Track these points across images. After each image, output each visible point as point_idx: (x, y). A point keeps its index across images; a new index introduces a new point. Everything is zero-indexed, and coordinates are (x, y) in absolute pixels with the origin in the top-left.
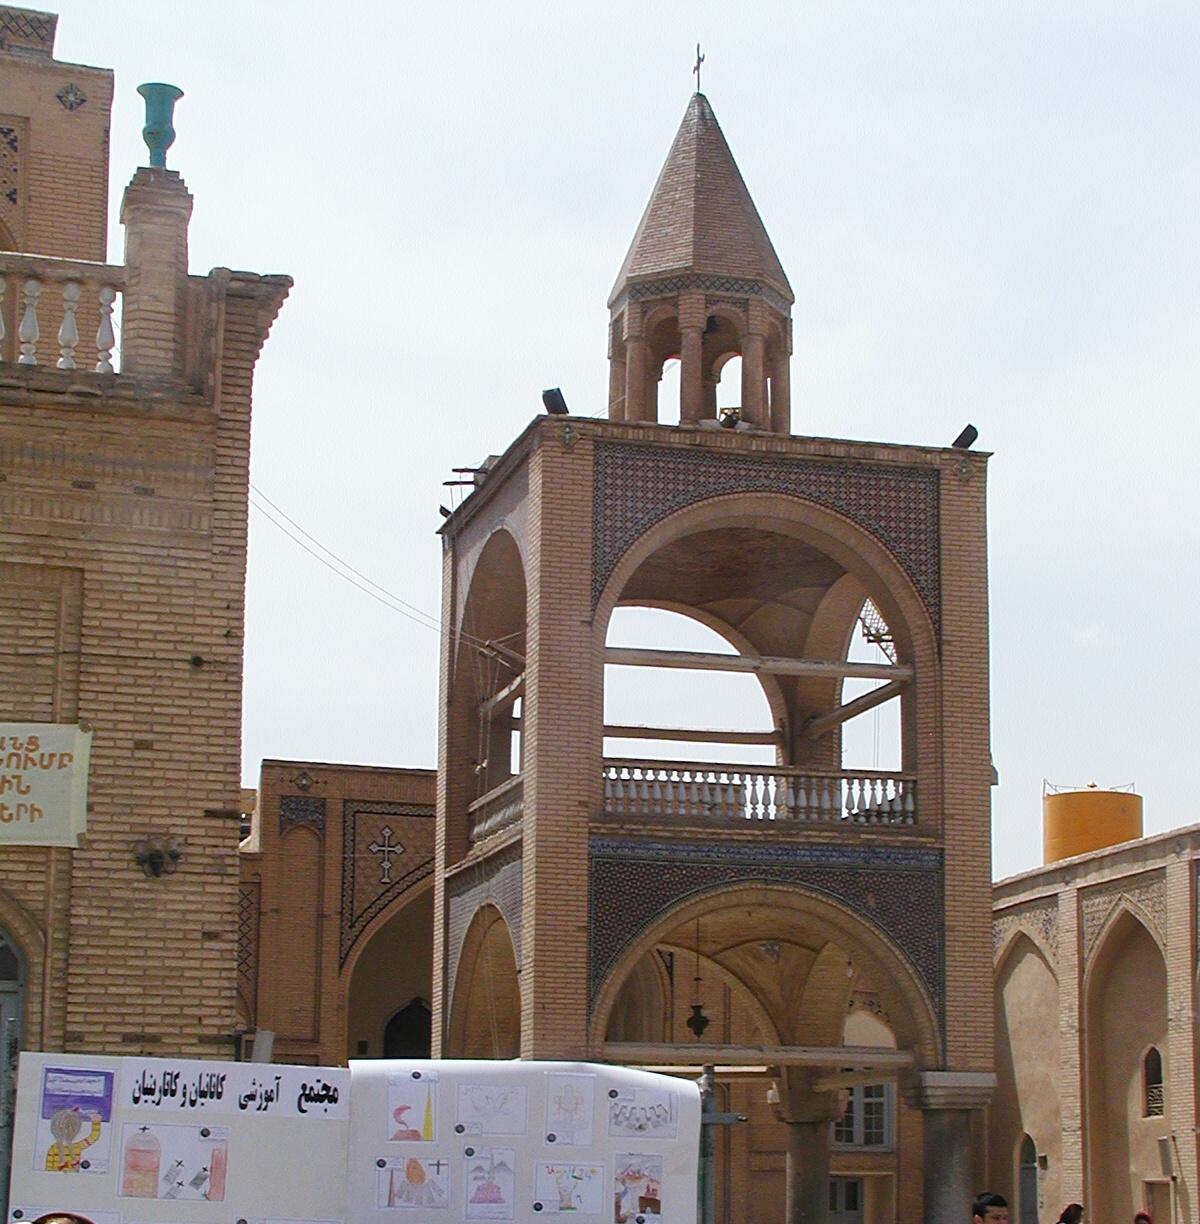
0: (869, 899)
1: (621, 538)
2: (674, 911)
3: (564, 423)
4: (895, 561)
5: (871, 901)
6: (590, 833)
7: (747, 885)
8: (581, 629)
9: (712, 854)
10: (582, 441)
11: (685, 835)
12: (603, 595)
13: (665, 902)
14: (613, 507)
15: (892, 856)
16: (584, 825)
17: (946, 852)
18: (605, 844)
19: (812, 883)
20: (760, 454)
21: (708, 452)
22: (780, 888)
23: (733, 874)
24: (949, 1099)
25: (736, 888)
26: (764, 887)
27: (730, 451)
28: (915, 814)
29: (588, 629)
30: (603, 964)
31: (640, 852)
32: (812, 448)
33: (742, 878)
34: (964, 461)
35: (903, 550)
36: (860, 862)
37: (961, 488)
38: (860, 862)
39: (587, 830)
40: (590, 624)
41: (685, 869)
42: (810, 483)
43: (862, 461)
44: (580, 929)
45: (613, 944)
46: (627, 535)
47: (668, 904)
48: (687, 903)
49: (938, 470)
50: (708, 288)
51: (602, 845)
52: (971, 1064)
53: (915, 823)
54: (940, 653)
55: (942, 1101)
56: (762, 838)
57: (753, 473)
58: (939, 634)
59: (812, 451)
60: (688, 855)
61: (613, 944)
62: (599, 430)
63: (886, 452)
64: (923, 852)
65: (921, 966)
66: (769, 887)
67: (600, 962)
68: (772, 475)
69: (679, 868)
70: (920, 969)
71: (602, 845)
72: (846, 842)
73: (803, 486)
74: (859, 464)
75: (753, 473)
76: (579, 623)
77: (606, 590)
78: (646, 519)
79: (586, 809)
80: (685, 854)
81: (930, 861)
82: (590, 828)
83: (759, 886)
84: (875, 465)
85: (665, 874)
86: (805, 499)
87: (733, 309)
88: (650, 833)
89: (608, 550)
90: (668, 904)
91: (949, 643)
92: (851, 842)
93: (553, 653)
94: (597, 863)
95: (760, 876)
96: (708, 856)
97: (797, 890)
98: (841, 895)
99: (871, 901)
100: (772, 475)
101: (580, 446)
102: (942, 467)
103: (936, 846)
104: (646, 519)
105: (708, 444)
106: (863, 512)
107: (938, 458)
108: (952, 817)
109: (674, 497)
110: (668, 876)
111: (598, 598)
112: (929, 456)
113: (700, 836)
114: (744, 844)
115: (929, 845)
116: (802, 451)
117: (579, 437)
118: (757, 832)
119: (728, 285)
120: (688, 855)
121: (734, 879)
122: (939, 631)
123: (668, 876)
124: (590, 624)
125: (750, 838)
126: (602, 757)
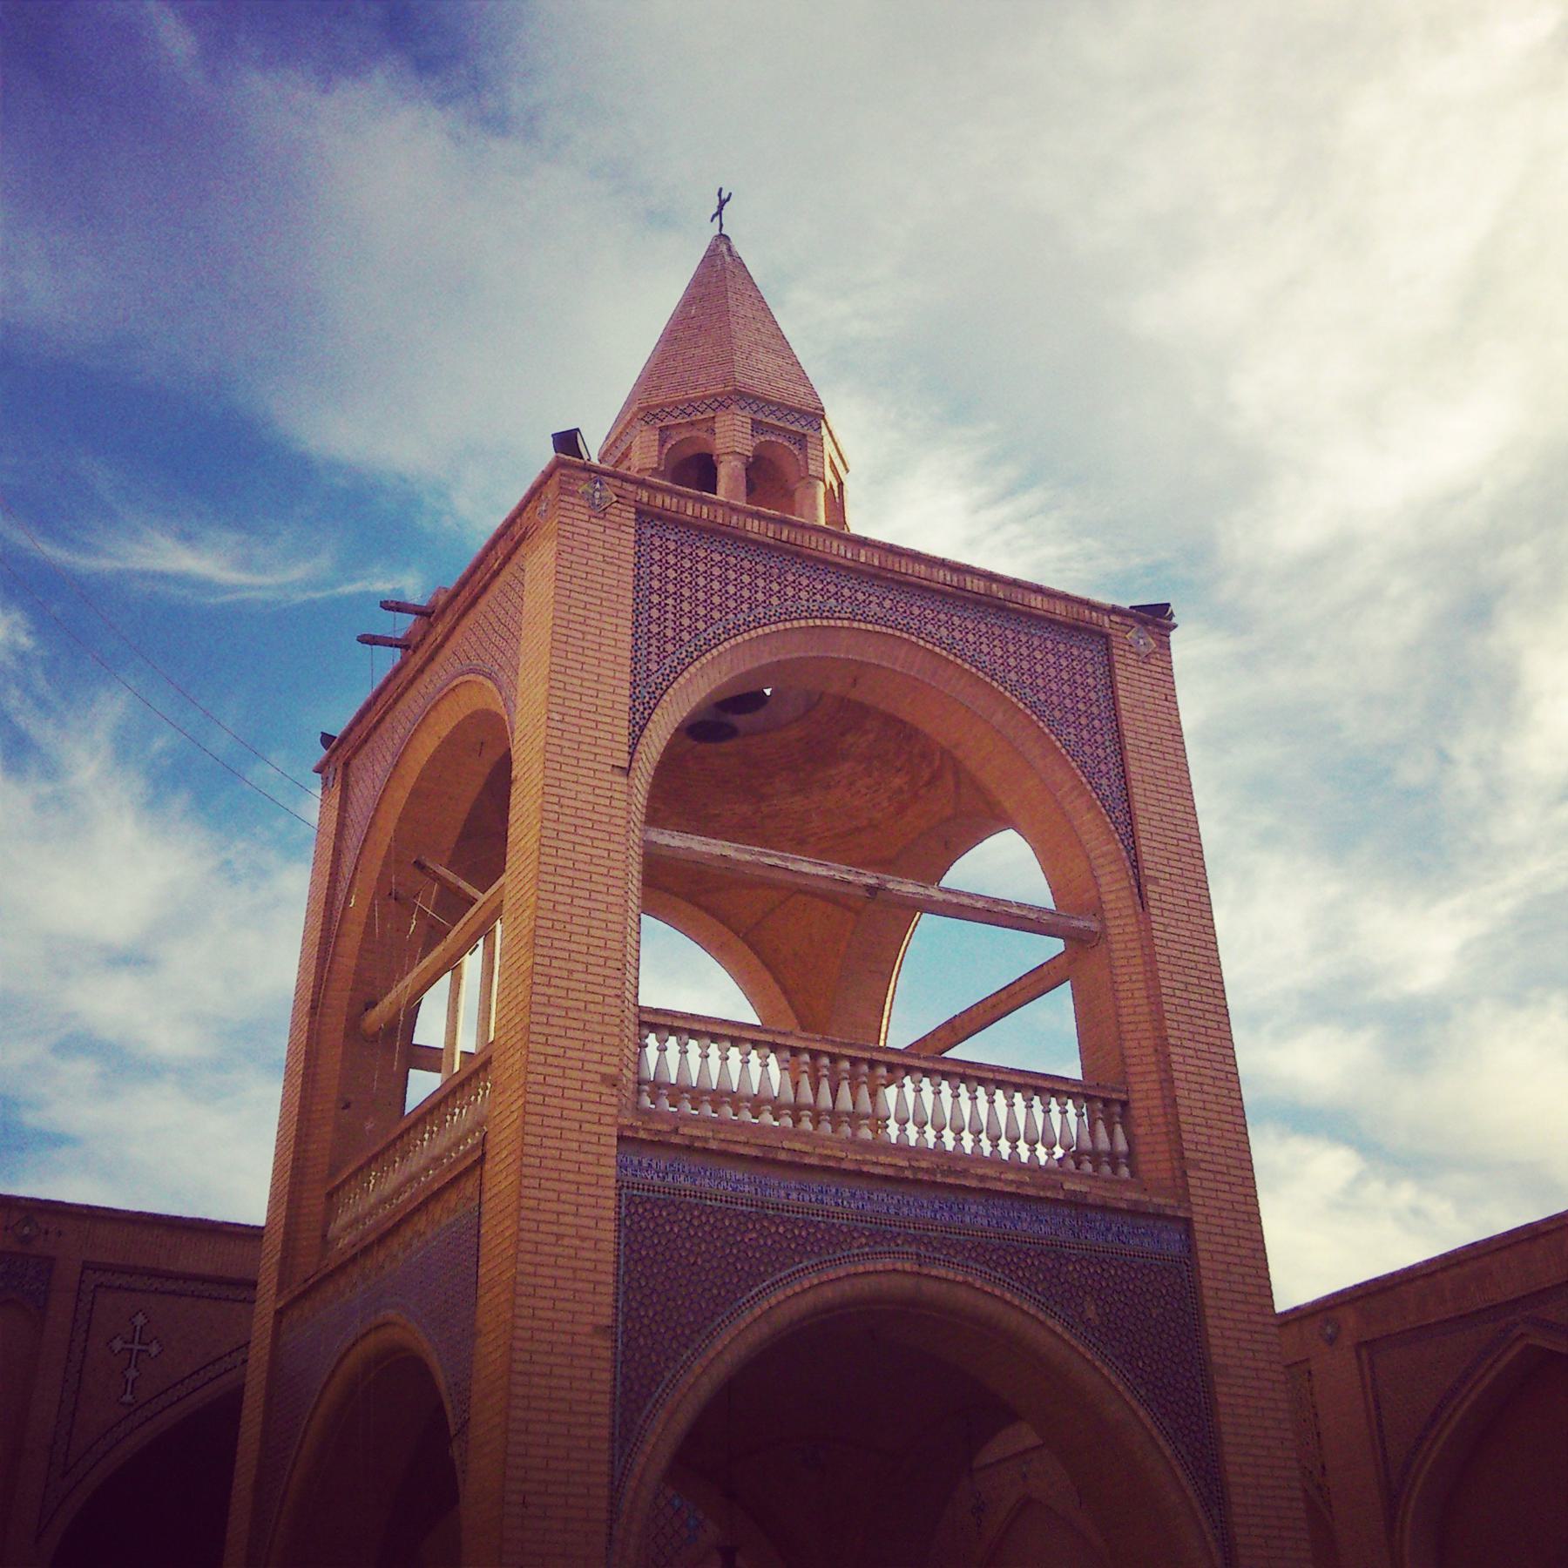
0: (1086, 1305)
1: (674, 653)
2: (765, 1306)
4: (1063, 751)
5: (1091, 1312)
6: (620, 1138)
8: (610, 777)
12: (646, 732)
14: (662, 607)
15: (1114, 1229)
16: (608, 1120)
17: (1197, 1226)
18: (645, 1165)
20: (873, 571)
22: (942, 1272)
23: (863, 1240)
26: (916, 1268)
28: (1130, 1155)
29: (624, 780)
35: (1072, 737)
39: (614, 1131)
40: (627, 771)
41: (783, 1222)
47: (756, 1290)
51: (640, 1163)
53: (1132, 1174)
54: (1141, 895)
57: (861, 597)
58: (1137, 867)
59: (941, 579)
64: (1159, 1224)
71: (640, 1163)
72: (1042, 1194)
73: (929, 626)
76: (609, 769)
77: (650, 725)
79: (615, 1091)
82: (621, 1127)
83: (907, 1267)
87: (786, 444)
88: (724, 1146)
89: (653, 667)
90: (756, 1290)
92: (1049, 1194)
99: (1091, 1312)
100: (887, 604)
103: (1181, 1214)
104: (710, 630)
106: (1013, 676)
109: (750, 609)
115: (1169, 1212)
116: (928, 577)
122: (1136, 863)
124: (627, 771)
126: (636, 1005)
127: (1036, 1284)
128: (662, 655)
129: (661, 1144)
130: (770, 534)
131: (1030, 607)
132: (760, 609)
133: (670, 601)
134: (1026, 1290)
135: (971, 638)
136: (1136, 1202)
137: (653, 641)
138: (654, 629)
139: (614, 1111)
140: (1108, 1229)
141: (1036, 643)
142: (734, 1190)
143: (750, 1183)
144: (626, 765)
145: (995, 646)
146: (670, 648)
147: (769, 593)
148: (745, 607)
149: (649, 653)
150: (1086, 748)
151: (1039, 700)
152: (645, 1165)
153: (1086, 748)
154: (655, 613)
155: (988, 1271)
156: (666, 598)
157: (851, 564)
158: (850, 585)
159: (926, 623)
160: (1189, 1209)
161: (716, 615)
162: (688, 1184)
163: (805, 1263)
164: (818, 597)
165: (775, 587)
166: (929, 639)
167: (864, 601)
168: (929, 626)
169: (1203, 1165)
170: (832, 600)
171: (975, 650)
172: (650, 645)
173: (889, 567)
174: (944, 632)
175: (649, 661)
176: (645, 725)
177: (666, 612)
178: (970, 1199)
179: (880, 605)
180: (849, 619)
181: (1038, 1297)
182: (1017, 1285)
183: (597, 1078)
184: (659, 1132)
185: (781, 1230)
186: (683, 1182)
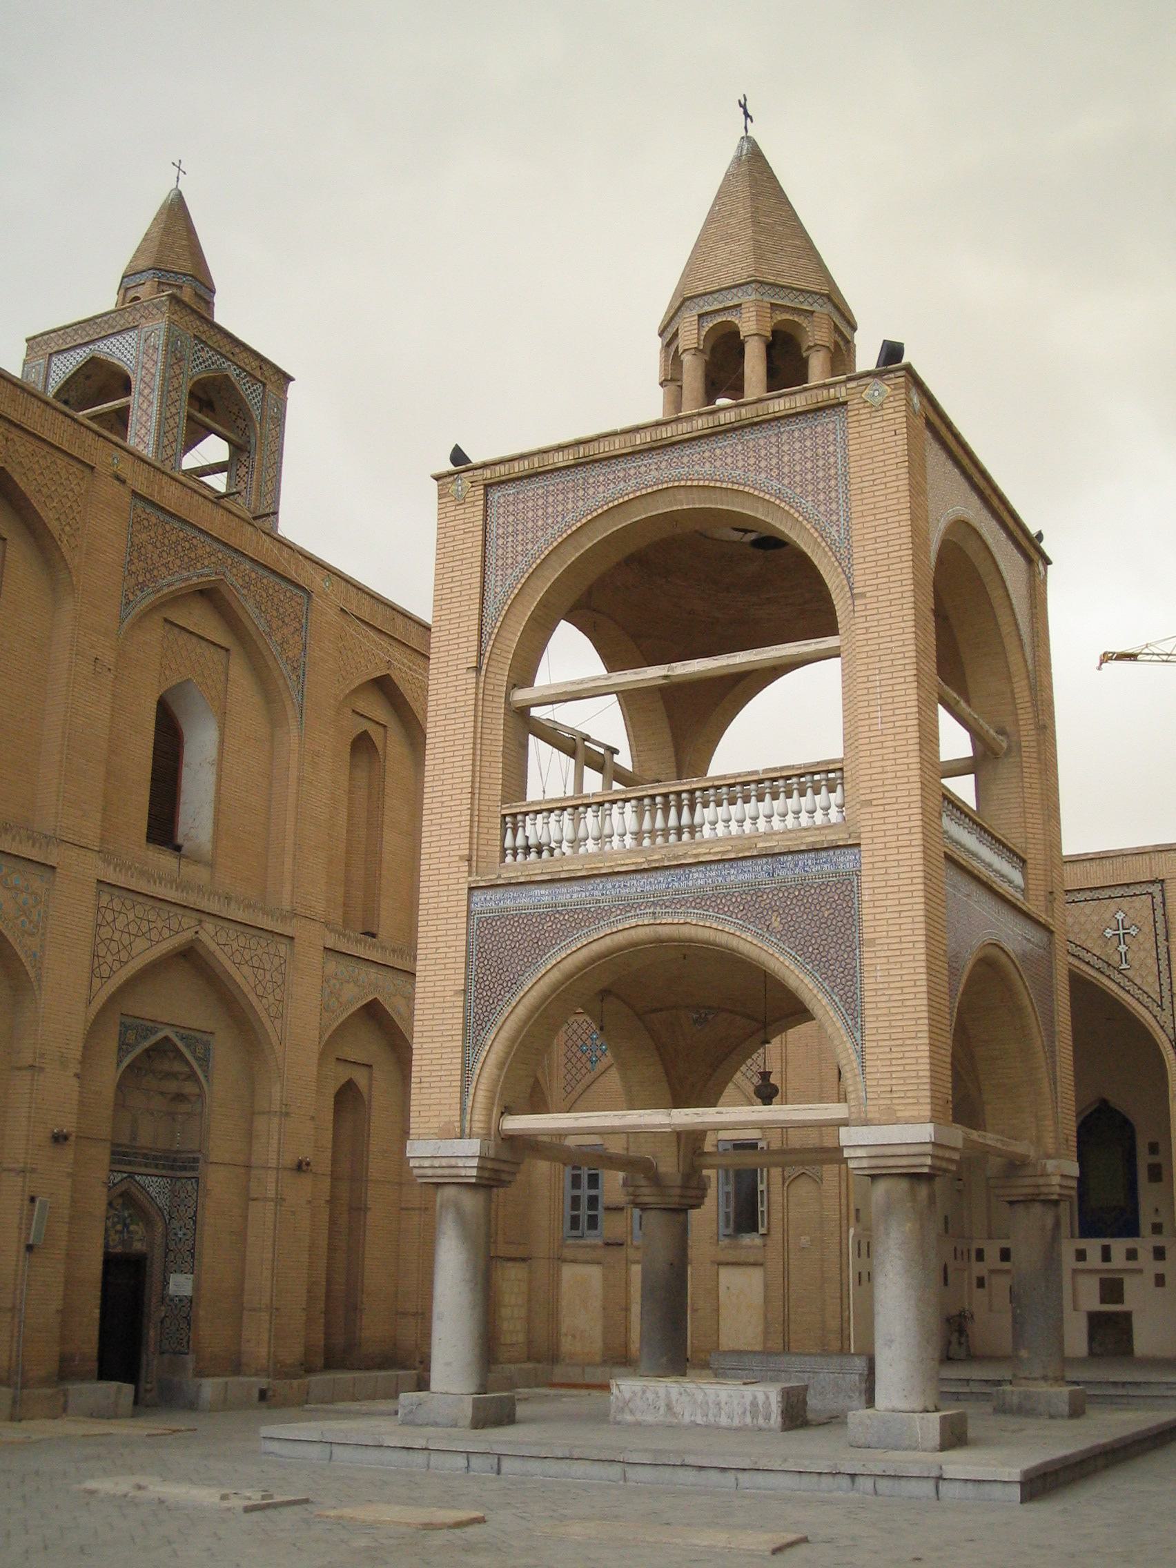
8: (466, 676)
11: (563, 875)
13: (545, 954)
14: (505, 545)
15: (801, 864)
19: (707, 910)
20: (646, 446)
26: (652, 922)
30: (483, 1029)
31: (523, 901)
35: (810, 503)
37: (873, 415)
38: (763, 876)
39: (466, 886)
41: (568, 913)
44: (457, 992)
45: (493, 1006)
46: (518, 570)
52: (899, 1114)
55: (865, 1164)
56: (645, 866)
57: (643, 469)
61: (493, 1006)
63: (782, 401)
67: (480, 1027)
70: (837, 999)
73: (696, 467)
75: (643, 469)
78: (536, 547)
82: (470, 883)
88: (528, 879)
89: (498, 590)
93: (440, 707)
94: (479, 920)
95: (648, 911)
97: (689, 920)
100: (663, 465)
101: (472, 494)
104: (536, 547)
107: (843, 389)
109: (563, 519)
112: (832, 391)
125: (633, 868)
129: (492, 886)
130: (571, 457)
133: (510, 539)
135: (729, 460)
139: (466, 874)
144: (474, 665)
146: (510, 571)
148: (559, 519)
153: (822, 508)
154: (500, 551)
155: (702, 912)
157: (630, 450)
165: (581, 493)
168: (696, 467)
169: (874, 803)
178: (694, 870)
181: (737, 921)
183: (457, 858)
185: (566, 917)
186: (509, 903)
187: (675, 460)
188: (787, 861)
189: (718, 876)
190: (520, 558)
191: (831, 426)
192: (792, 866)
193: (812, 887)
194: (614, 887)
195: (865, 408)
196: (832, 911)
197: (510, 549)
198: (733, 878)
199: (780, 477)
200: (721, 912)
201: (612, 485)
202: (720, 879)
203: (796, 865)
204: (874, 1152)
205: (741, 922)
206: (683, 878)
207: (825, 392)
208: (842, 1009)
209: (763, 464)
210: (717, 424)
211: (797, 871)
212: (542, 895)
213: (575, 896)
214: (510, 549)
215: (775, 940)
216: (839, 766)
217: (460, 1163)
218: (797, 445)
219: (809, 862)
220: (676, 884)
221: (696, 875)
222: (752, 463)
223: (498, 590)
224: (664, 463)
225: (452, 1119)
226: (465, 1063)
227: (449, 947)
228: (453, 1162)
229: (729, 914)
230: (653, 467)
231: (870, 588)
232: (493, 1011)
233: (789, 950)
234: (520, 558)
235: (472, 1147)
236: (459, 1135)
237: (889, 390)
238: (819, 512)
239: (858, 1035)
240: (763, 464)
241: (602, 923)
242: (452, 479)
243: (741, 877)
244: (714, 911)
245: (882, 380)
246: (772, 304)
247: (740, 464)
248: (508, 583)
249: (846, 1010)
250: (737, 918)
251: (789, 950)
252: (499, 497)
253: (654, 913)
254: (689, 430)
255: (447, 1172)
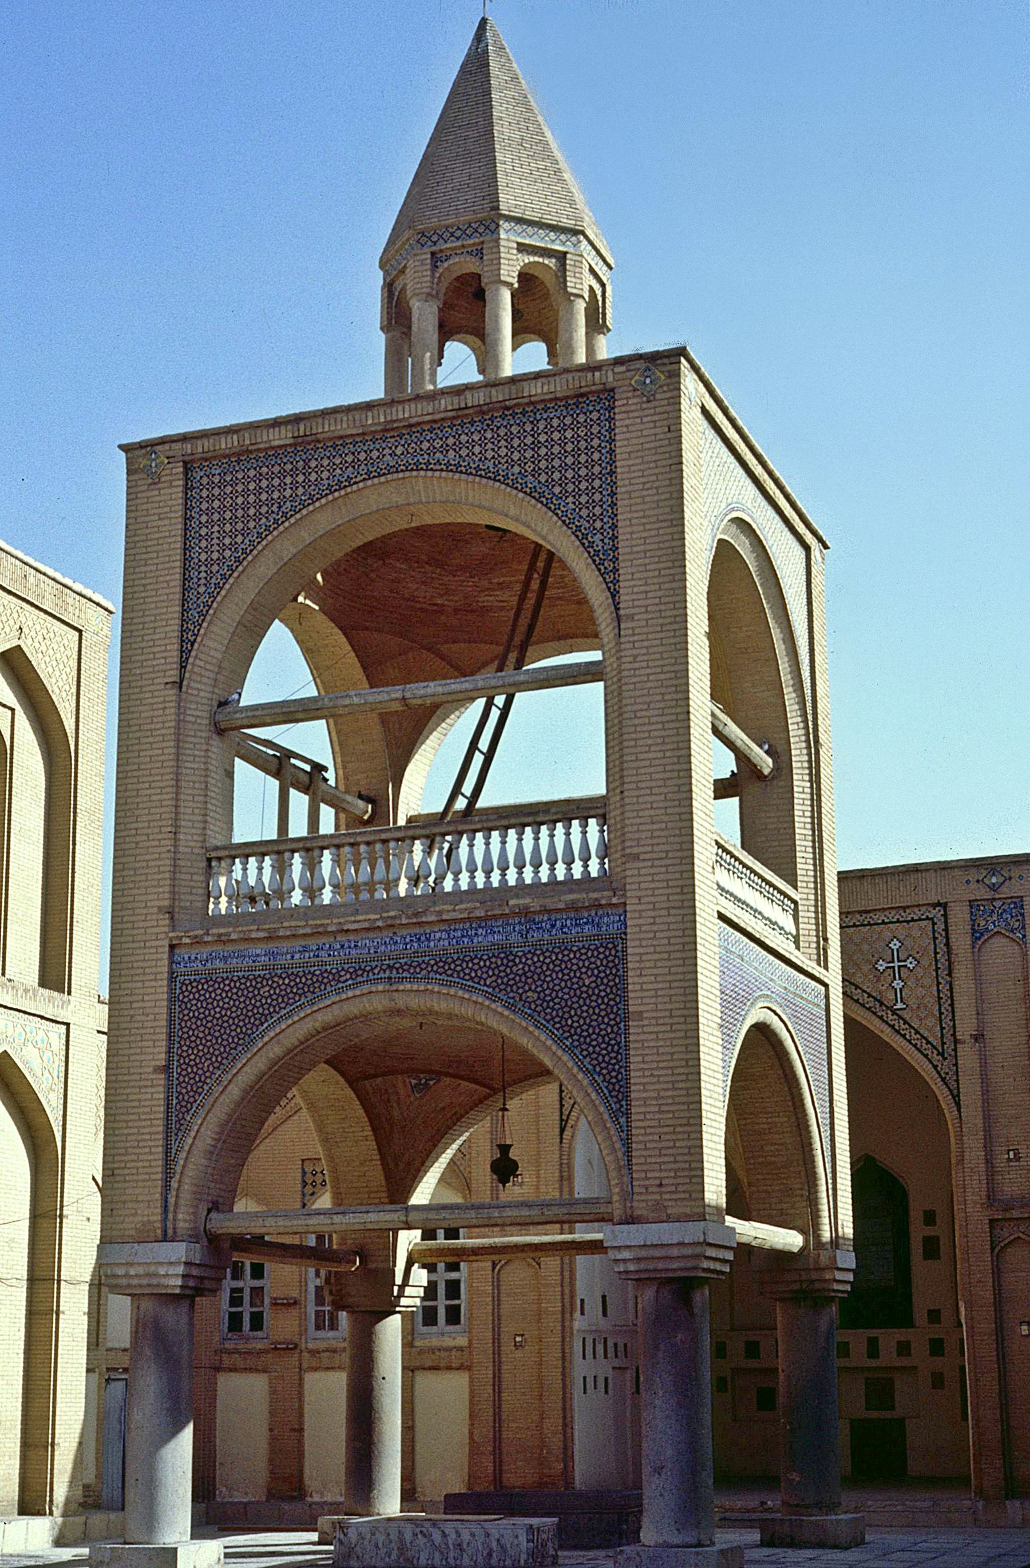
3: (149, 449)
7: (366, 988)
9: (322, 953)
10: (170, 466)
12: (196, 646)
13: (262, 1024)
14: (209, 536)
16: (163, 936)
18: (193, 958)
19: (452, 975)
20: (379, 428)
21: (319, 441)
22: (408, 986)
24: (642, 1266)
25: (350, 994)
26: (387, 987)
27: (342, 433)
30: (188, 1111)
32: (444, 403)
33: (360, 979)
34: (648, 369)
36: (514, 938)
38: (514, 938)
39: (166, 943)
41: (288, 976)
42: (432, 451)
43: (507, 403)
47: (266, 1025)
48: (290, 1022)
49: (612, 390)
50: (435, 243)
51: (189, 958)
56: (380, 924)
60: (293, 957)
62: (188, 447)
64: (600, 912)
65: (599, 1074)
66: (394, 988)
68: (399, 452)
69: (280, 977)
70: (599, 1079)
73: (438, 455)
74: (508, 408)
75: (375, 454)
80: (289, 957)
81: (609, 925)
83: (380, 988)
84: (528, 404)
85: (263, 987)
86: (442, 470)
91: (631, 617)
95: (382, 975)
96: (318, 956)
98: (488, 986)
102: (615, 384)
103: (614, 901)
104: (246, 541)
105: (314, 431)
106: (516, 469)
108: (636, 857)
109: (280, 507)
110: (267, 988)
111: (190, 651)
113: (302, 931)
114: (364, 935)
117: (166, 461)
118: (373, 917)
119: (458, 233)
120: (293, 957)
121: (350, 982)
123: (267, 988)
125: (366, 925)
127: (485, 980)
128: (210, 574)
131: (530, 396)
132: (288, 504)
133: (216, 528)
134: (476, 985)
136: (573, 902)
137: (203, 568)
138: (203, 557)
140: (553, 926)
141: (541, 427)
142: (254, 962)
143: (265, 955)
145: (499, 448)
146: (215, 568)
147: (295, 486)
148: (275, 508)
149: (199, 579)
150: (584, 513)
151: (540, 482)
152: (193, 958)
153: (584, 513)
154: (204, 544)
156: (212, 526)
158: (365, 448)
159: (435, 453)
160: (624, 895)
161: (252, 525)
162: (222, 965)
163: (303, 1000)
164: (338, 471)
165: (301, 478)
166: (438, 467)
167: (378, 457)
168: (438, 455)
170: (350, 469)
171: (480, 460)
172: (200, 573)
173: (394, 418)
174: (451, 453)
175: (199, 586)
176: (195, 640)
177: (212, 539)
179: (393, 454)
180: (364, 479)
181: (486, 988)
182: (468, 983)
183: (155, 910)
184: (196, 937)
186: (218, 964)
187: (413, 445)
188: (543, 921)
189: (463, 936)
190: (227, 553)
191: (595, 416)
192: (548, 926)
193: (571, 950)
194: (342, 946)
195: (634, 397)
196: (593, 979)
197: (215, 541)
198: (480, 939)
199: (536, 473)
200: (467, 977)
201: (338, 471)
202: (466, 940)
203: (553, 926)
204: (643, 1253)
205: (490, 990)
206: (423, 938)
207: (590, 375)
208: (606, 1091)
209: (516, 456)
210: (463, 405)
211: (554, 933)
212: (258, 955)
213: (297, 956)
214: (215, 541)
215: (529, 1011)
216: (600, 811)
217: (162, 1271)
218: (556, 436)
219: (568, 922)
220: (416, 945)
221: (438, 935)
222: (503, 454)
223: (202, 589)
224: (400, 448)
225: (152, 1218)
226: (167, 1151)
227: (148, 1015)
228: (152, 1269)
229: (476, 980)
230: (387, 451)
231: (637, 610)
232: (200, 1090)
233: (544, 1023)
234: (227, 553)
235: (179, 1251)
236: (160, 1238)
237: (663, 377)
238: (581, 517)
239: (623, 1120)
240: (516, 456)
241: (329, 989)
242: (143, 451)
243: (490, 938)
244: (459, 977)
245: (656, 365)
246: (518, 244)
247: (490, 454)
248: (213, 581)
249: (610, 1092)
250: (485, 985)
251: (544, 1023)
252: (201, 477)
253: (390, 978)
254: (430, 411)
255: (144, 1282)
